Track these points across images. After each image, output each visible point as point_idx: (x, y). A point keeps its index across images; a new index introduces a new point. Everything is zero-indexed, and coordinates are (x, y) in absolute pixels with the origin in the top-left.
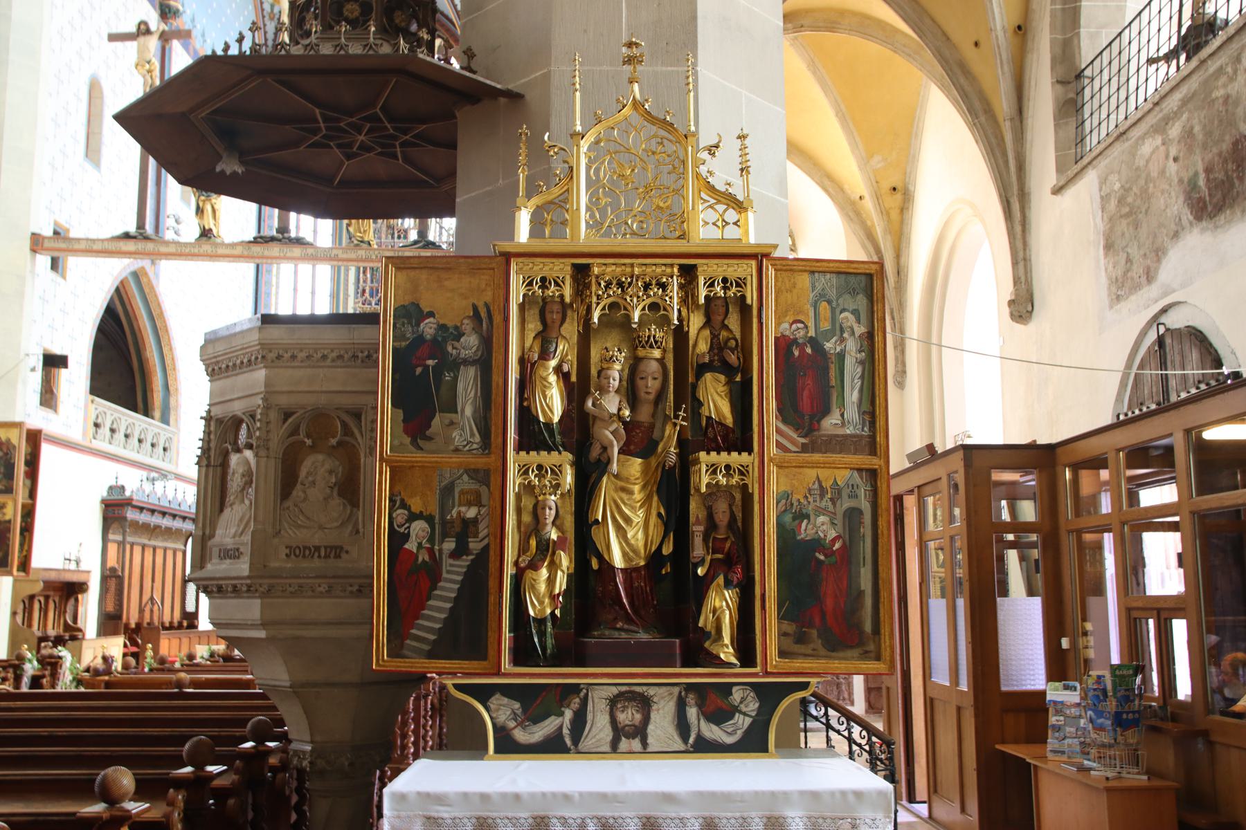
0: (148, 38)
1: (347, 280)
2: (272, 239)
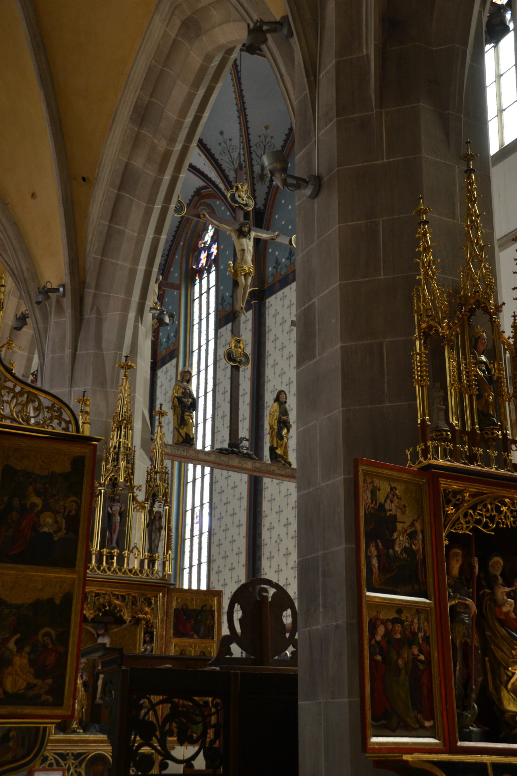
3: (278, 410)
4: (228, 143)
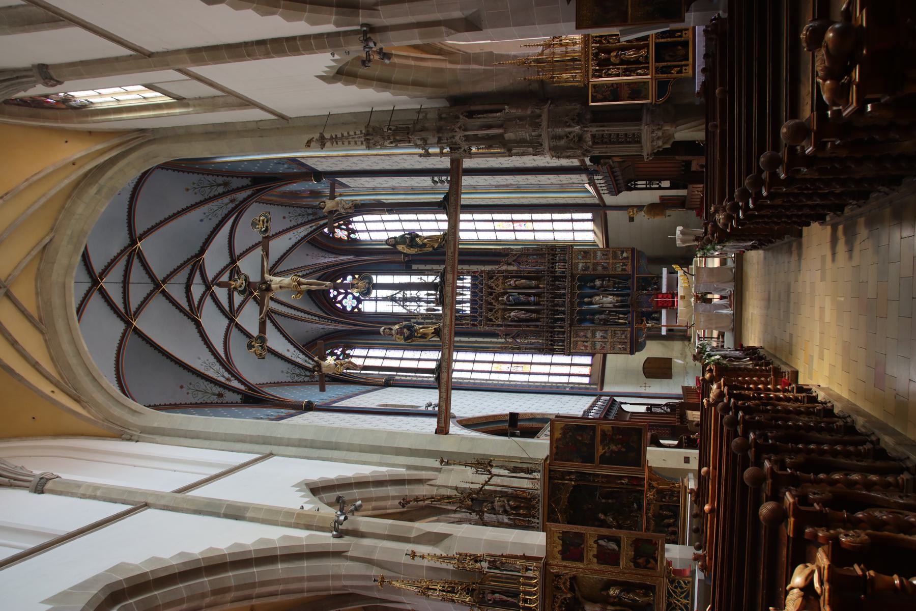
0: (323, 366)
1: (466, 342)
2: (441, 292)
3: (402, 246)
4: (207, 214)
